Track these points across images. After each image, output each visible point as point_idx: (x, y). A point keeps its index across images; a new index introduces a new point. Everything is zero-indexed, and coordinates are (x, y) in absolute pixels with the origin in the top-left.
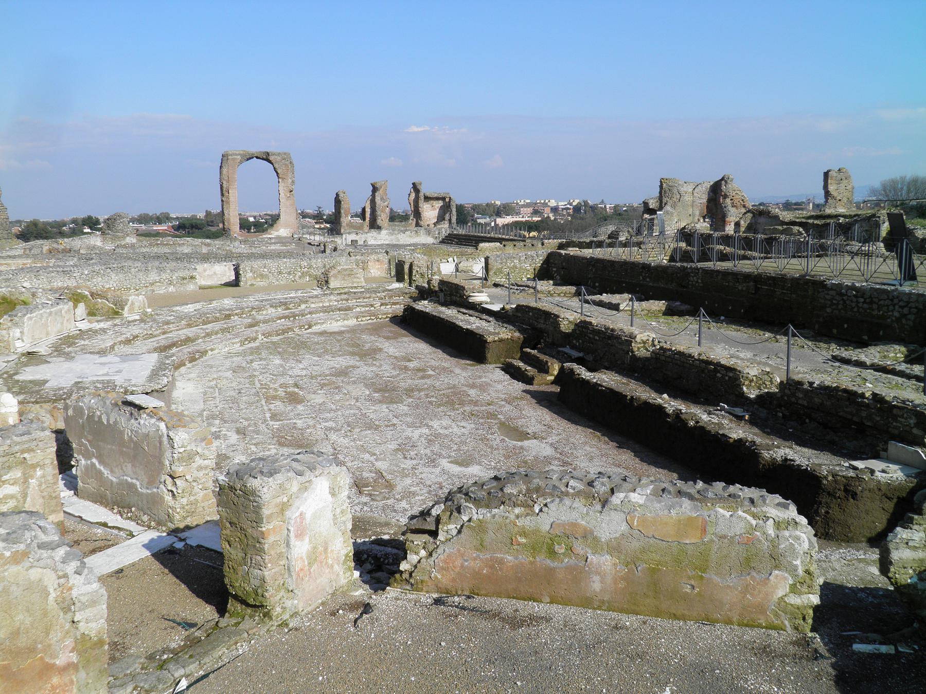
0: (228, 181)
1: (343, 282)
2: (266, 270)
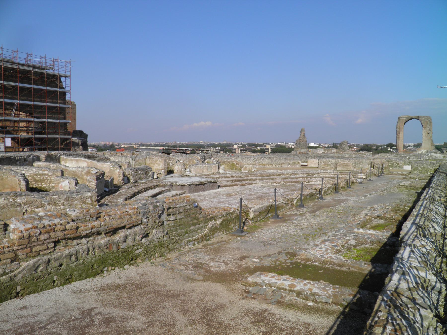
0: (399, 129)
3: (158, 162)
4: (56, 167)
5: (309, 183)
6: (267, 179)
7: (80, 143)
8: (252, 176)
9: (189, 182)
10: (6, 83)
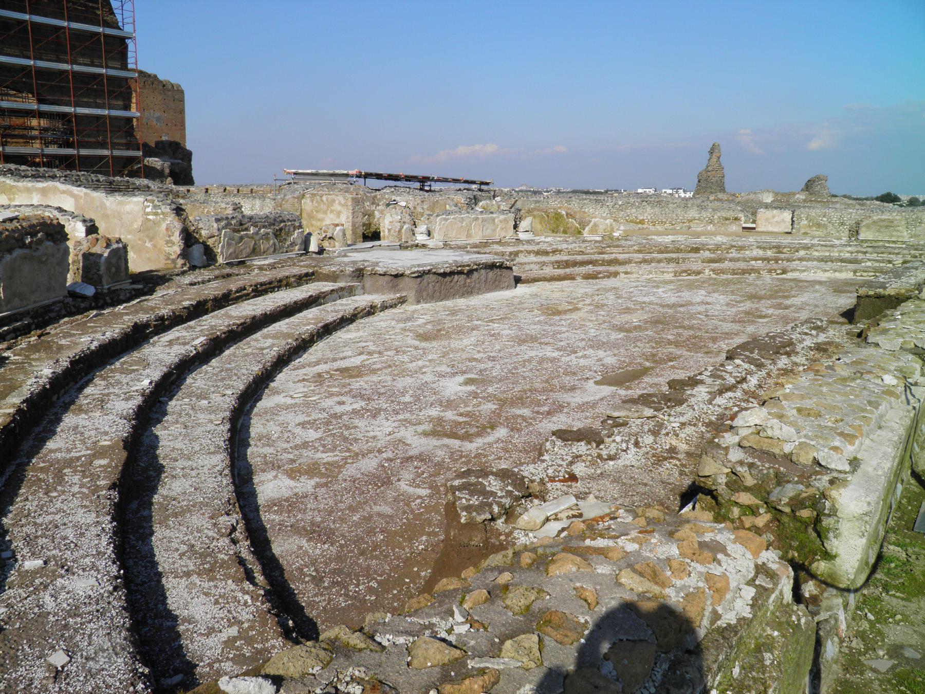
1: (877, 234)
2: (825, 219)
3: (337, 207)
5: (784, 276)
6: (659, 261)
7: (167, 171)
8: (615, 250)
9: (419, 266)
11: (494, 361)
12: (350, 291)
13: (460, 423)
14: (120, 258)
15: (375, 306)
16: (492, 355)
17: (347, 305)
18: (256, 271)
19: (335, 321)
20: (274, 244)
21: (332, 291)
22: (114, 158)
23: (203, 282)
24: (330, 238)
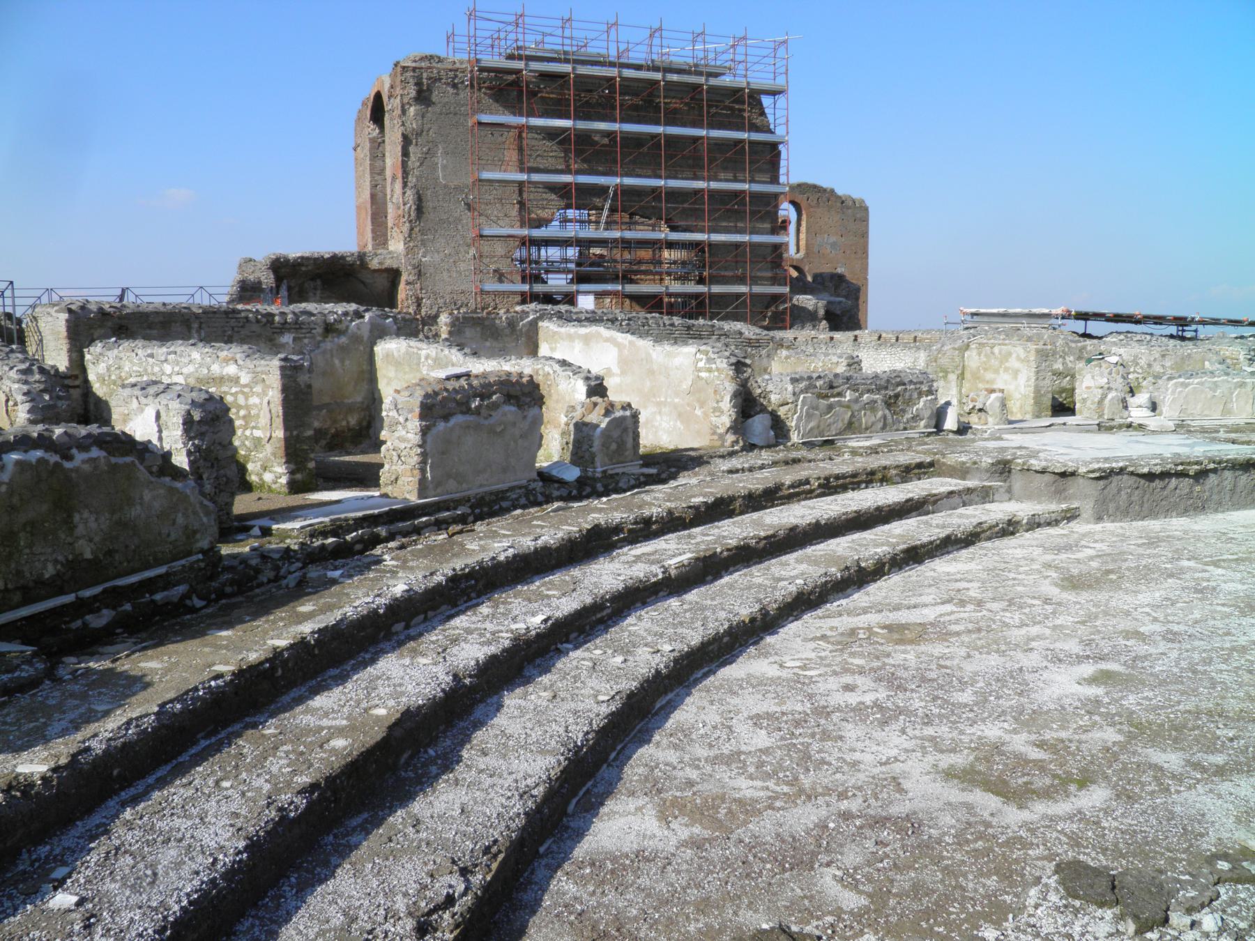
3: (1013, 363)
4: (435, 360)
7: (821, 312)
9: (1106, 460)
10: (582, 125)
11: (1172, 641)
12: (985, 495)
13: (1027, 761)
14: (625, 430)
15: (1018, 523)
16: (1176, 628)
17: (968, 517)
18: (846, 456)
19: (931, 543)
20: (885, 417)
21: (951, 493)
22: (753, 296)
23: (751, 470)
24: (980, 410)
